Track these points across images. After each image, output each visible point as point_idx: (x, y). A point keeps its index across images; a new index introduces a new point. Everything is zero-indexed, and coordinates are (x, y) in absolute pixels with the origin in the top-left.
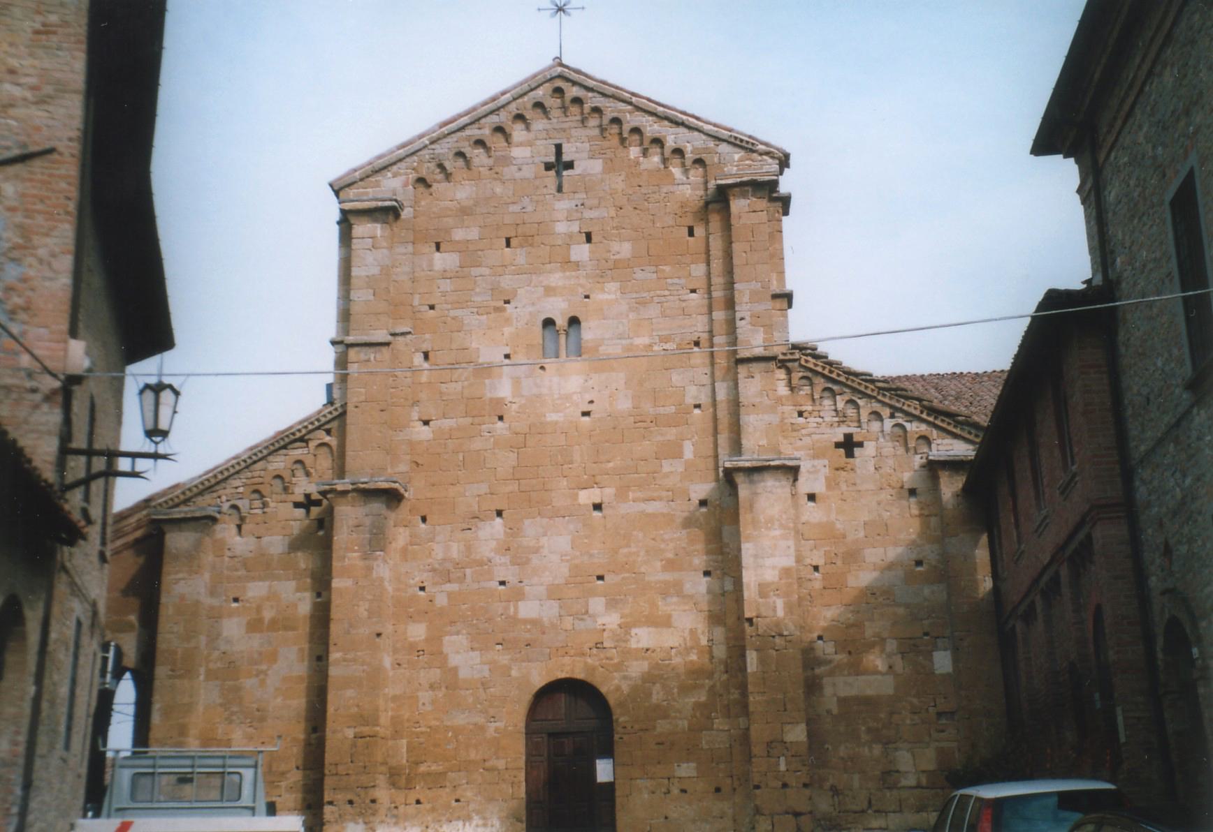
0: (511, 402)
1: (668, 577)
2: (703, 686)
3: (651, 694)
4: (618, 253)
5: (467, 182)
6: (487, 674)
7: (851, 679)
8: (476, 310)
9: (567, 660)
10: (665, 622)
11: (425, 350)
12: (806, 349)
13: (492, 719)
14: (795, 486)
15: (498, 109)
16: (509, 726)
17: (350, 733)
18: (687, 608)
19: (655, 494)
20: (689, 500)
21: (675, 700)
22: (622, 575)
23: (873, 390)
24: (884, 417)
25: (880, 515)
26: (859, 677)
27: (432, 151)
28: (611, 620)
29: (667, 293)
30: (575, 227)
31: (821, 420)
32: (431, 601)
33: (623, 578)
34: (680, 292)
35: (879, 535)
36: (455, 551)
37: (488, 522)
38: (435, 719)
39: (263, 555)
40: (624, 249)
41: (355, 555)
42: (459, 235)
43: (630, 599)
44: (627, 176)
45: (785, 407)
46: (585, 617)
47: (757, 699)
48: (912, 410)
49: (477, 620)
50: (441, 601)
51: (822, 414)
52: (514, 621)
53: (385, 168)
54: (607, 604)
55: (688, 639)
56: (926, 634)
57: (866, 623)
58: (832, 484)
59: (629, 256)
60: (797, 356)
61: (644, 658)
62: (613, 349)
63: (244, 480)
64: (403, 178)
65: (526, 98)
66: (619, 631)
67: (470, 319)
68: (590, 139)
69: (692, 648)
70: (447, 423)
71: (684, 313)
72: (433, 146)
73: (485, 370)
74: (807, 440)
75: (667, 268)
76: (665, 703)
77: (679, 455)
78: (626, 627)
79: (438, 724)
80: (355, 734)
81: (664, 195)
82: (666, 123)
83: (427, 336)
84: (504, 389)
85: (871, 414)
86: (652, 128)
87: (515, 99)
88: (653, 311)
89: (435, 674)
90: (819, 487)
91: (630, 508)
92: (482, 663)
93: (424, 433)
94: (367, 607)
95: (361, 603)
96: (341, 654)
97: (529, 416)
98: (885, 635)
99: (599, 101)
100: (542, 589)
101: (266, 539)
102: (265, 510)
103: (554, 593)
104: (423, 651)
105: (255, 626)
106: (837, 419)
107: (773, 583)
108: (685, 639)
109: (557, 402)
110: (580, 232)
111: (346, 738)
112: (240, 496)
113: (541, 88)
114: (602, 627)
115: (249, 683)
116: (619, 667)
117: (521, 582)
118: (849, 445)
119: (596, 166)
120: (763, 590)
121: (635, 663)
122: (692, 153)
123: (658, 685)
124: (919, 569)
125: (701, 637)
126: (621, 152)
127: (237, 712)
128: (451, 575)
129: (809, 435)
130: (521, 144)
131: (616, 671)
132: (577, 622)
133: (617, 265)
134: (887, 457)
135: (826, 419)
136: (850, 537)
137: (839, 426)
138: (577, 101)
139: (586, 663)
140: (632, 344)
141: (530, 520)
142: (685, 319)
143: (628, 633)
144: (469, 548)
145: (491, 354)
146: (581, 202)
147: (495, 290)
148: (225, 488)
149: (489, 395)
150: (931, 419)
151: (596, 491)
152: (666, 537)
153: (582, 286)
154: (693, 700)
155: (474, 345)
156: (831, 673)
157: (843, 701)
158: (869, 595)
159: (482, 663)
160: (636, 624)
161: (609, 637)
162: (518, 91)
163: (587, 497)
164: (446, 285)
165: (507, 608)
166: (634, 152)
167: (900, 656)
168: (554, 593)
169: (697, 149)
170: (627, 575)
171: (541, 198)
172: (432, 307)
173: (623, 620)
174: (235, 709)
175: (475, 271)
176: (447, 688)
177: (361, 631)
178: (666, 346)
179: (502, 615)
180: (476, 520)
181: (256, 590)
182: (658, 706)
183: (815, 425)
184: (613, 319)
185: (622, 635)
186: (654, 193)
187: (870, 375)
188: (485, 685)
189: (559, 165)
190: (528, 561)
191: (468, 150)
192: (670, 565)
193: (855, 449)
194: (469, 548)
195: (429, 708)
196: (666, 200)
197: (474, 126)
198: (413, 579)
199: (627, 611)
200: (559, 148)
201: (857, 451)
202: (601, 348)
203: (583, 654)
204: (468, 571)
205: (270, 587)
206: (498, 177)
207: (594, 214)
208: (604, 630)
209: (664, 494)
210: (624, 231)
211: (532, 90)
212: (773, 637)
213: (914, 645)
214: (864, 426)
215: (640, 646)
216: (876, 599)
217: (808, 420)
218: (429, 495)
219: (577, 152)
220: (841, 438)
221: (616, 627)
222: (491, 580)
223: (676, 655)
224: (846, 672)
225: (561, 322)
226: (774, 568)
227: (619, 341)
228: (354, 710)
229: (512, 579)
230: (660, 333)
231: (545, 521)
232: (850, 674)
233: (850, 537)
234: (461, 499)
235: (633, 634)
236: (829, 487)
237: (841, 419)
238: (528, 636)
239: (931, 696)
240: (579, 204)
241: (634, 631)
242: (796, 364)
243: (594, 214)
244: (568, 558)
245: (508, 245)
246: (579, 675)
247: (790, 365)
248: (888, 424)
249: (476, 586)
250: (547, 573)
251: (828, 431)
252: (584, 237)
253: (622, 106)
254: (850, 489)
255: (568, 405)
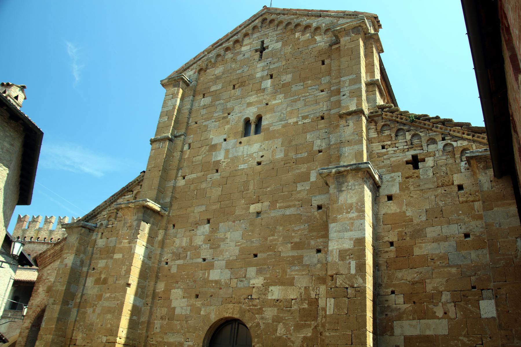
0: (223, 162)
1: (295, 253)
2: (310, 325)
3: (277, 330)
4: (285, 80)
5: (221, 66)
6: (188, 312)
7: (414, 322)
8: (214, 120)
9: (231, 306)
10: (291, 283)
11: (189, 143)
12: (385, 108)
13: (187, 340)
14: (378, 191)
15: (237, 33)
16: (196, 345)
17: (104, 339)
18: (303, 273)
19: (291, 203)
20: (312, 205)
21: (291, 335)
22: (268, 253)
23: (429, 125)
24: (438, 141)
25: (437, 204)
26: (421, 321)
27: (207, 57)
28: (258, 281)
29: (308, 94)
30: (265, 73)
31: (397, 149)
32: (169, 270)
33: (268, 255)
34: (315, 92)
35: (436, 218)
36: (185, 242)
37: (202, 226)
38: (160, 337)
39: (107, 247)
40: (288, 78)
41: (126, 241)
42: (213, 89)
43: (271, 268)
44: (293, 45)
45: (373, 144)
46: (244, 279)
47: (332, 334)
48: (456, 134)
49: (189, 280)
50: (174, 270)
51: (397, 145)
52: (207, 281)
53: (188, 68)
54: (257, 272)
55: (303, 293)
56: (474, 287)
57: (427, 281)
58: (403, 187)
59: (290, 80)
60: (380, 113)
61: (275, 306)
62: (278, 127)
63: (107, 212)
64: (195, 70)
65: (250, 26)
66: (262, 288)
67: (211, 124)
68: (277, 35)
69: (305, 300)
70: (194, 176)
71: (317, 102)
72: (208, 55)
73: (214, 148)
74: (387, 162)
75: (310, 82)
76: (284, 336)
77: (308, 179)
78: (266, 286)
79: (161, 340)
80: (106, 340)
81: (310, 49)
82: (313, 18)
83: (192, 136)
84: (220, 156)
85: (428, 140)
86: (305, 21)
87: (245, 27)
88: (300, 104)
89: (164, 311)
90: (395, 190)
91: (274, 213)
92: (188, 306)
93: (181, 182)
94: (125, 269)
95: (124, 267)
96: (109, 294)
97: (230, 168)
98: (441, 288)
99: (282, 17)
100: (223, 263)
101: (110, 239)
102: (113, 225)
103: (229, 265)
104: (161, 297)
105: (97, 281)
106: (407, 147)
107: (349, 249)
108: (301, 294)
109: (245, 159)
110: (267, 75)
111: (102, 342)
112: (105, 219)
113: (257, 20)
114: (252, 286)
115: (89, 310)
116: (260, 311)
117: (213, 259)
118: (415, 162)
119: (279, 45)
120: (343, 254)
121: (269, 309)
122: (325, 27)
123: (281, 324)
124: (467, 239)
125: (312, 292)
126: (292, 37)
127: (82, 325)
128: (181, 255)
129: (389, 159)
130: (246, 45)
131: (257, 314)
132: (239, 283)
133: (284, 86)
134: (441, 166)
135: (400, 148)
136: (415, 222)
137: (408, 151)
138: (272, 21)
139: (241, 307)
140: (287, 123)
141: (223, 223)
142: (316, 105)
143: (267, 289)
144: (191, 240)
145: (216, 139)
146: (270, 62)
147: (225, 110)
148: (100, 216)
149: (213, 160)
150: (470, 137)
151: (259, 205)
152: (296, 229)
153: (265, 99)
154: (303, 335)
155: (211, 137)
156: (399, 318)
157: (408, 339)
158: (429, 260)
159: (188, 306)
160: (275, 284)
161: (256, 292)
162: (247, 23)
163: (253, 208)
164: (203, 112)
165: (204, 274)
166: (297, 35)
167: (453, 304)
168: (229, 265)
169: (328, 24)
170: (270, 253)
171: (252, 64)
172: (196, 123)
173: (265, 281)
174: (82, 323)
175: (217, 103)
176: (168, 319)
177: (120, 282)
178: (306, 121)
179: (201, 278)
180: (197, 225)
181: (101, 264)
182: (280, 338)
183: (393, 152)
184: (279, 112)
185: (264, 291)
186: (306, 50)
187: (426, 116)
188: (187, 318)
189: (263, 49)
190: (219, 246)
191: (222, 53)
192: (297, 246)
193: (419, 163)
194: (191, 240)
195: (158, 330)
196: (311, 51)
197: (227, 42)
198: (163, 258)
199: (268, 276)
200: (263, 42)
201: (420, 165)
202: (271, 128)
203: (240, 303)
204: (189, 253)
205: (107, 262)
206: (234, 60)
207: (276, 65)
208: (254, 287)
209: (297, 203)
210: (289, 69)
211: (253, 22)
212: (347, 288)
213: (464, 296)
214: (425, 148)
215: (274, 298)
216: (434, 263)
217: (387, 150)
218: (178, 213)
219: (270, 42)
220: (410, 158)
221: (260, 285)
222: (199, 257)
223: (294, 304)
224: (411, 317)
225: (253, 118)
226: (351, 239)
227: (281, 123)
228: (109, 326)
229: (209, 257)
230: (303, 115)
231: (230, 223)
232: (414, 319)
233: (415, 222)
234: (192, 214)
235: (270, 290)
236: (401, 189)
237: (410, 146)
238: (212, 290)
239: (478, 336)
240: (269, 63)
241: (271, 288)
242: (380, 118)
243: (276, 65)
244: (239, 244)
245: (234, 88)
246: (236, 316)
247: (376, 119)
248: (441, 144)
249: (191, 261)
250: (227, 253)
251: (401, 154)
252: (269, 76)
253: (292, 16)
254: (416, 189)
255: (250, 159)
